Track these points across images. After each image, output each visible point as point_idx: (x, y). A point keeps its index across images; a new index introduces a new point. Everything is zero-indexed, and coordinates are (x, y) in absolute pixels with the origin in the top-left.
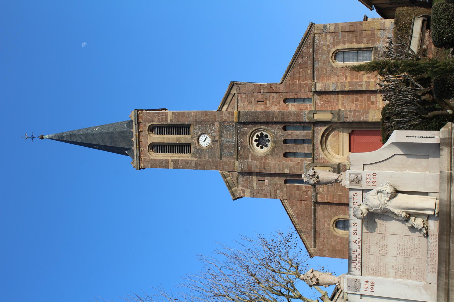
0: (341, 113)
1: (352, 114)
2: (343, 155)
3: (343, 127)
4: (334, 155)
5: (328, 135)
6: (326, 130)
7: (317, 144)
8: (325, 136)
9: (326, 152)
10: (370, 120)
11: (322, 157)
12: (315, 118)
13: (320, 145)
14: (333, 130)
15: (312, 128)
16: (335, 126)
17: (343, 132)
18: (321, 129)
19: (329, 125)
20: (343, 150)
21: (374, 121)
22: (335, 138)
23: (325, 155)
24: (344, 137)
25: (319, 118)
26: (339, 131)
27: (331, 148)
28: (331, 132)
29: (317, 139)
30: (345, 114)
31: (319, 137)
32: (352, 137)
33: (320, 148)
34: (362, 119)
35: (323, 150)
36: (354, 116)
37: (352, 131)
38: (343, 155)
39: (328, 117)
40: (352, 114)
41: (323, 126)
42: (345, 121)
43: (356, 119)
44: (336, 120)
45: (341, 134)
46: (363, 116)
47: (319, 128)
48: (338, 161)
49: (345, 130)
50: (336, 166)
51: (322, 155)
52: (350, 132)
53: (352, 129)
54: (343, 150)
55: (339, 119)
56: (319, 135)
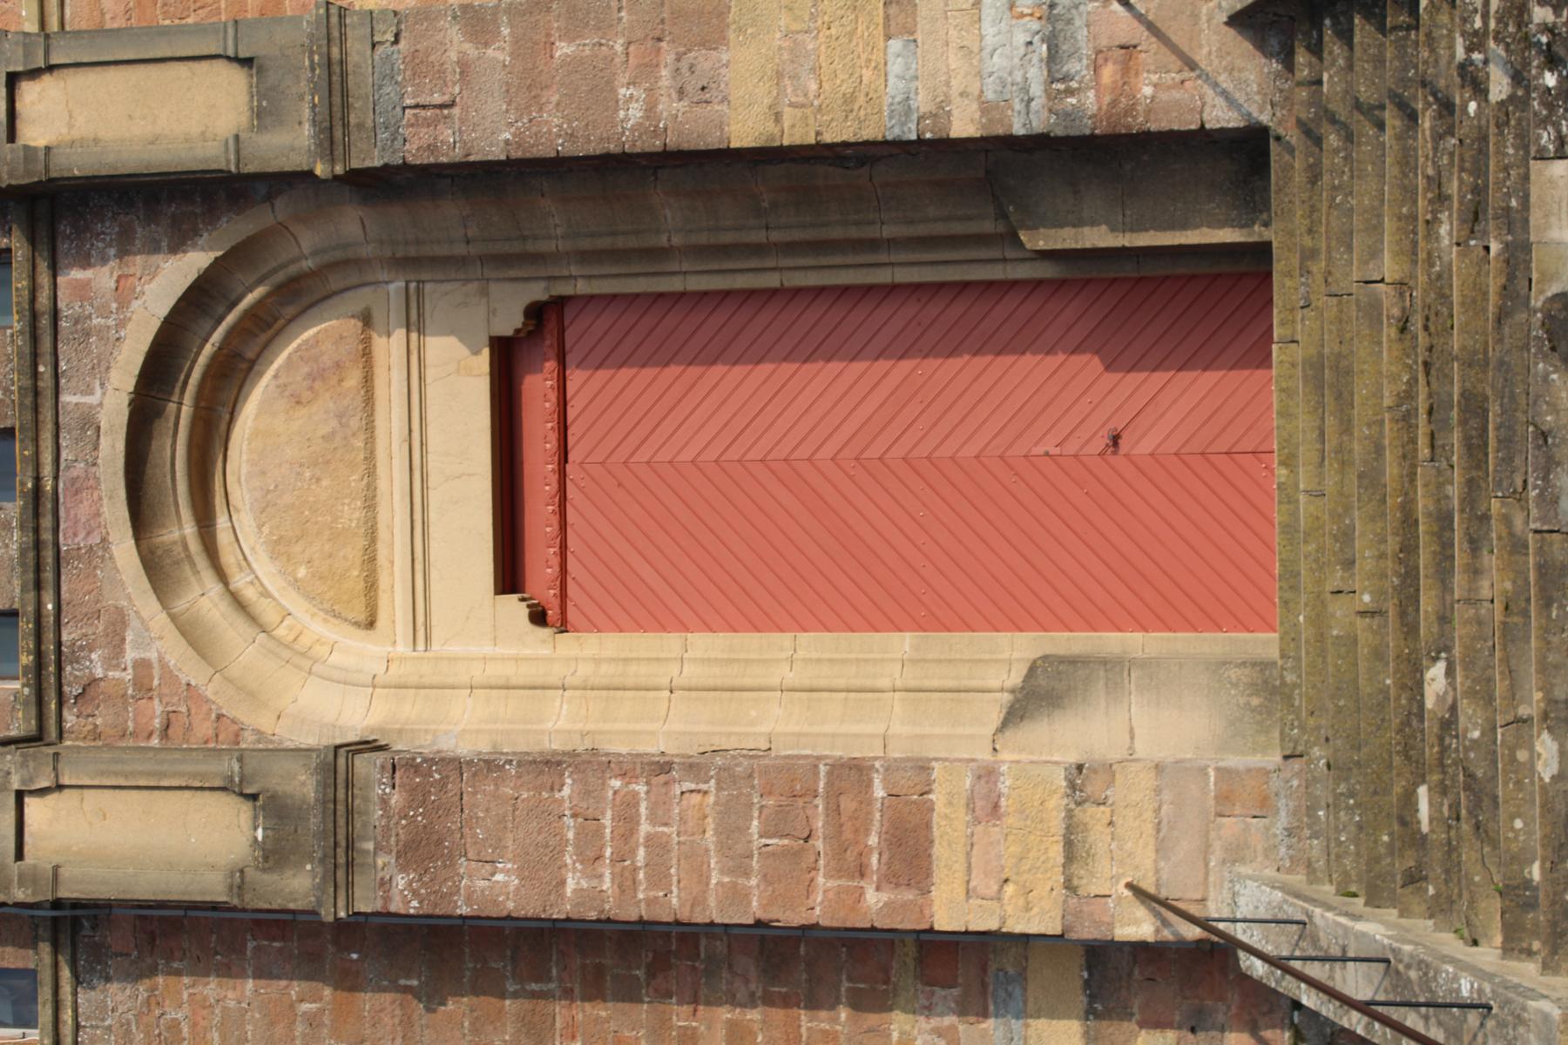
0: (357, 49)
1: (498, 53)
2: (421, 629)
3: (415, 263)
4: (314, 627)
5: (232, 373)
6: (199, 301)
7: (76, 490)
8: (189, 388)
9: (203, 597)
10: (745, 131)
11: (142, 666)
12: (34, 134)
13: (115, 510)
14: (298, 296)
15: (20, 282)
16: (306, 245)
17: (415, 323)
18: (124, 294)
19: (235, 229)
20: (419, 562)
21: (796, 132)
22: (319, 417)
23: (191, 632)
24: (442, 384)
25: (84, 126)
26: (367, 320)
27: (279, 548)
28: (264, 328)
29: (89, 423)
30: (419, 64)
31: (103, 395)
32: (537, 388)
33: (124, 550)
34: (638, 113)
35: (156, 568)
36: (527, 87)
37: (537, 313)
38: (421, 629)
39: (185, 115)
40: (498, 53)
41: (154, 248)
42: (418, 144)
43: (555, 129)
44: (291, 144)
45: (390, 347)
46: (648, 70)
47: (102, 277)
48: (354, 716)
49: (441, 295)
50: (303, 785)
51: (151, 634)
52: (509, 321)
53: (538, 292)
54: (419, 562)
55: (334, 125)
56: (101, 368)
